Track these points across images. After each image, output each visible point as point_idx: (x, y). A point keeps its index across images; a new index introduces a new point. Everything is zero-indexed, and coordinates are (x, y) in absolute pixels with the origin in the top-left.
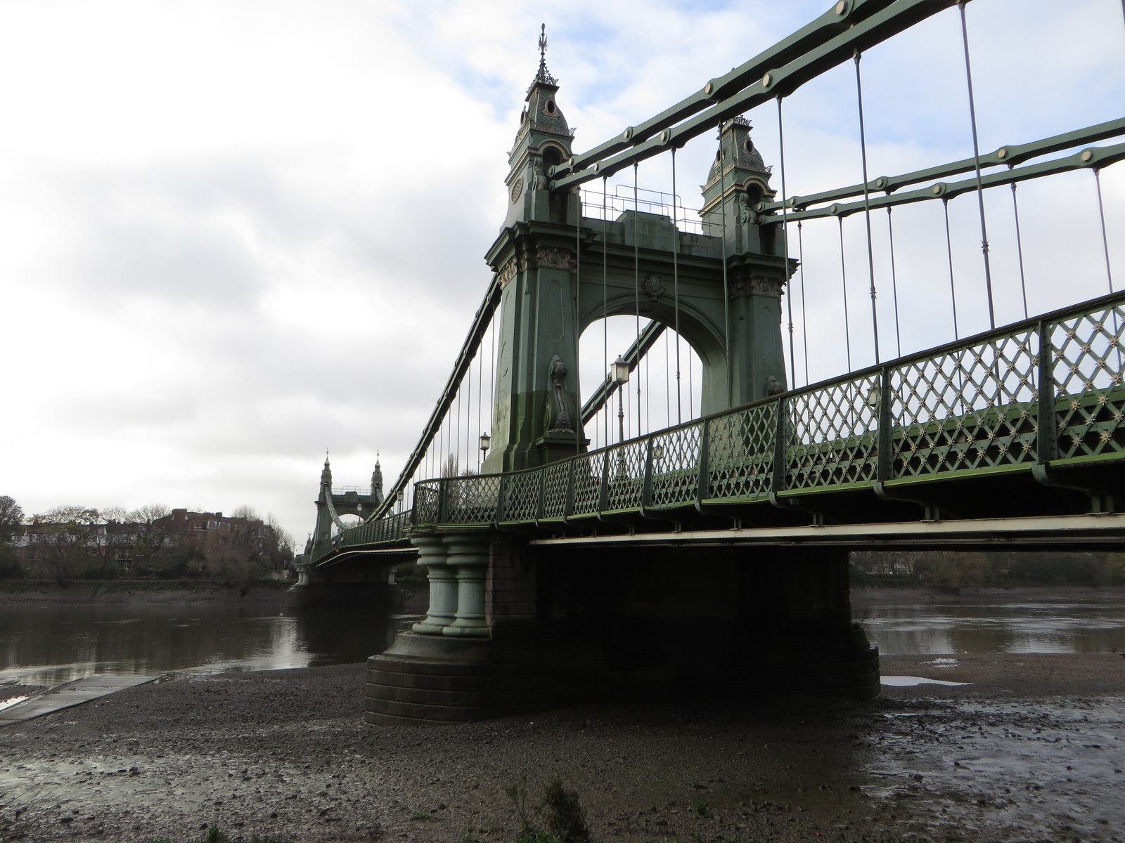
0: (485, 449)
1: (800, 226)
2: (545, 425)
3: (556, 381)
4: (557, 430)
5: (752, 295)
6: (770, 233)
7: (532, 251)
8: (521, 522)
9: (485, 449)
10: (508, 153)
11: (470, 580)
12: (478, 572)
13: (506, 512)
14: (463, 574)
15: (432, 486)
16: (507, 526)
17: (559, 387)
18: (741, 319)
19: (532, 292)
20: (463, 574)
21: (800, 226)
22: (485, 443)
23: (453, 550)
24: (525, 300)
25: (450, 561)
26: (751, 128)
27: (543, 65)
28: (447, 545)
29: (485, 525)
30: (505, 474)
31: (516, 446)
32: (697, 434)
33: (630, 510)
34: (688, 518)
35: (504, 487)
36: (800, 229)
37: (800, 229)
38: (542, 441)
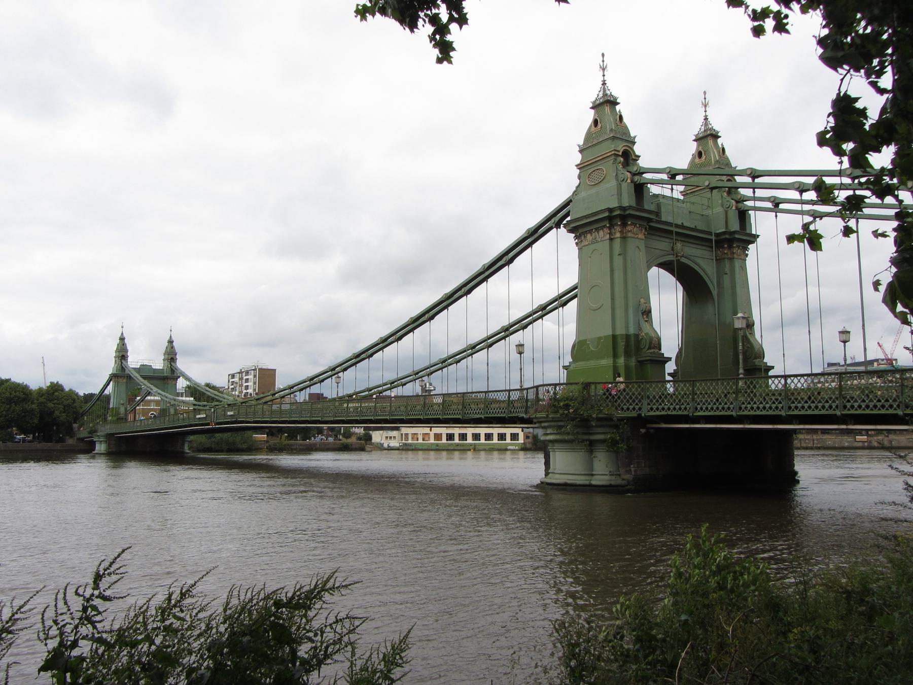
1: (776, 216)
3: (645, 317)
4: (652, 351)
5: (734, 258)
6: (743, 216)
7: (624, 225)
10: (579, 146)
12: (612, 446)
13: (650, 407)
16: (658, 416)
18: (726, 274)
21: (776, 216)
26: (720, 137)
27: (604, 84)
29: (634, 414)
36: (776, 218)
37: (776, 218)
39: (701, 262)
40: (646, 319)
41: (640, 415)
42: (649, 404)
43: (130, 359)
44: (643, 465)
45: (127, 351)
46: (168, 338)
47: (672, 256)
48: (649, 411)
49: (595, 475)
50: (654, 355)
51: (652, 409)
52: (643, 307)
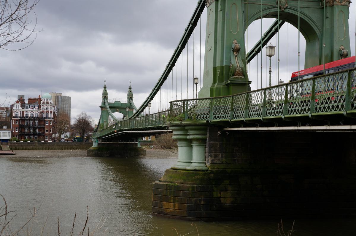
0: (196, 84)
2: (230, 75)
3: (235, 53)
5: (334, 5)
8: (222, 120)
9: (196, 84)
11: (199, 146)
12: (202, 142)
13: (214, 115)
14: (194, 144)
15: (180, 103)
17: (236, 56)
19: (223, 10)
20: (194, 144)
22: (196, 81)
23: (191, 132)
24: (220, 14)
25: (189, 137)
28: (187, 130)
29: (204, 121)
30: (211, 98)
31: (216, 85)
32: (309, 84)
33: (277, 117)
34: (305, 121)
35: (211, 104)
38: (229, 82)
39: (306, 11)
40: (236, 55)
41: (208, 121)
42: (214, 114)
43: (108, 98)
44: (220, 157)
45: (107, 94)
46: (104, 85)
47: (277, 9)
48: (214, 119)
49: (193, 163)
50: (236, 80)
51: (215, 117)
52: (235, 45)
